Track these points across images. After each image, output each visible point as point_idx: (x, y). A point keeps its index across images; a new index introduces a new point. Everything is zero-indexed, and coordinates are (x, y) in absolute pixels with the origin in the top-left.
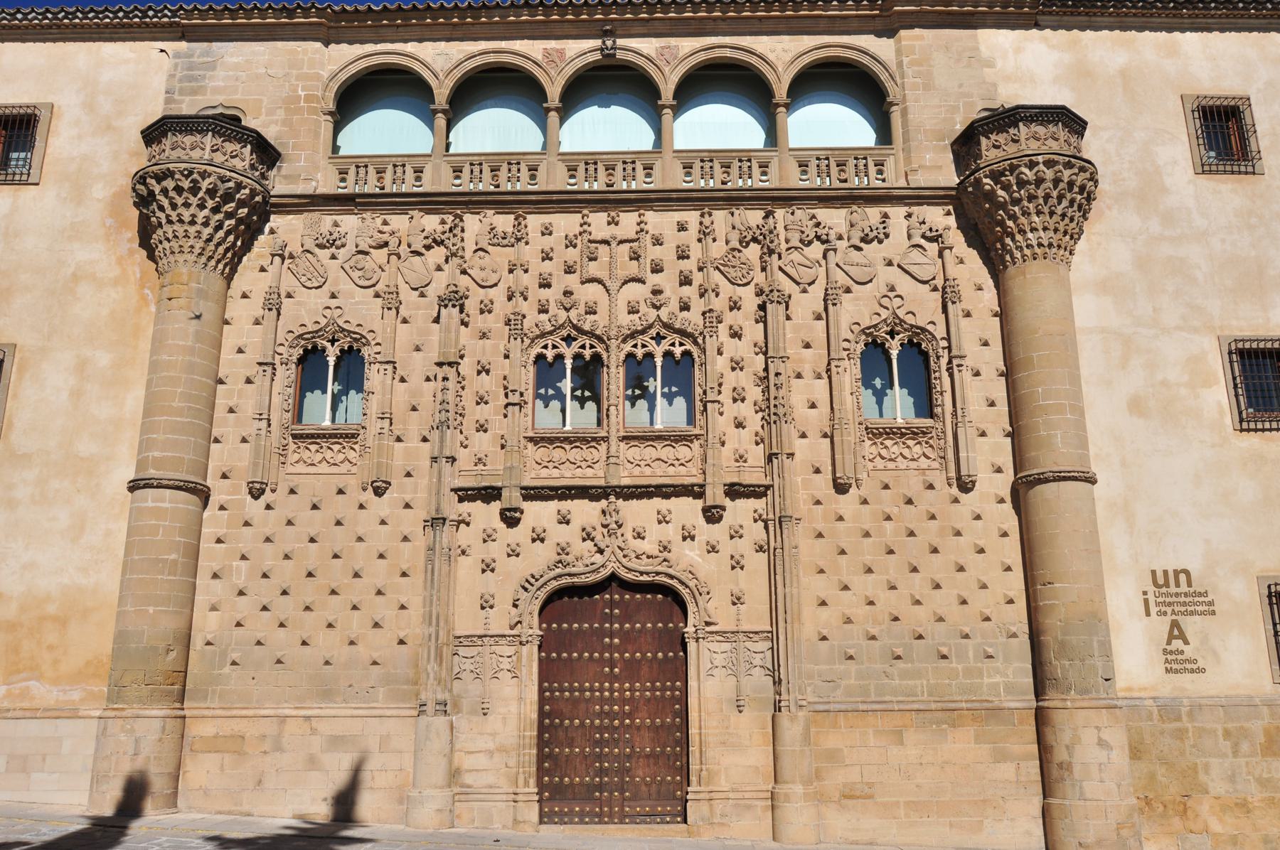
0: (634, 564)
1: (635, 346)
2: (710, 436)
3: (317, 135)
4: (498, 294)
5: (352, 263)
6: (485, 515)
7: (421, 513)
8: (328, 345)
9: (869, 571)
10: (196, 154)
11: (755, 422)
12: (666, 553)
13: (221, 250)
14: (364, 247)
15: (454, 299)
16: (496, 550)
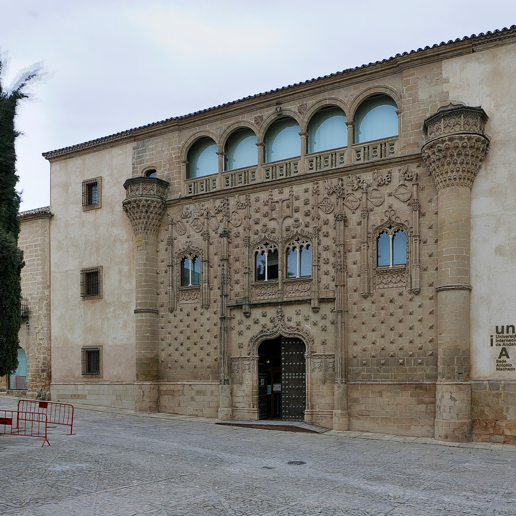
0: (287, 331)
1: (290, 245)
2: (314, 280)
3: (180, 172)
4: (241, 229)
5: (193, 224)
6: (238, 315)
7: (219, 315)
8: (188, 255)
9: (373, 330)
10: (137, 193)
11: (332, 271)
12: (298, 327)
13: (151, 226)
14: (196, 216)
15: (226, 234)
16: (243, 328)
